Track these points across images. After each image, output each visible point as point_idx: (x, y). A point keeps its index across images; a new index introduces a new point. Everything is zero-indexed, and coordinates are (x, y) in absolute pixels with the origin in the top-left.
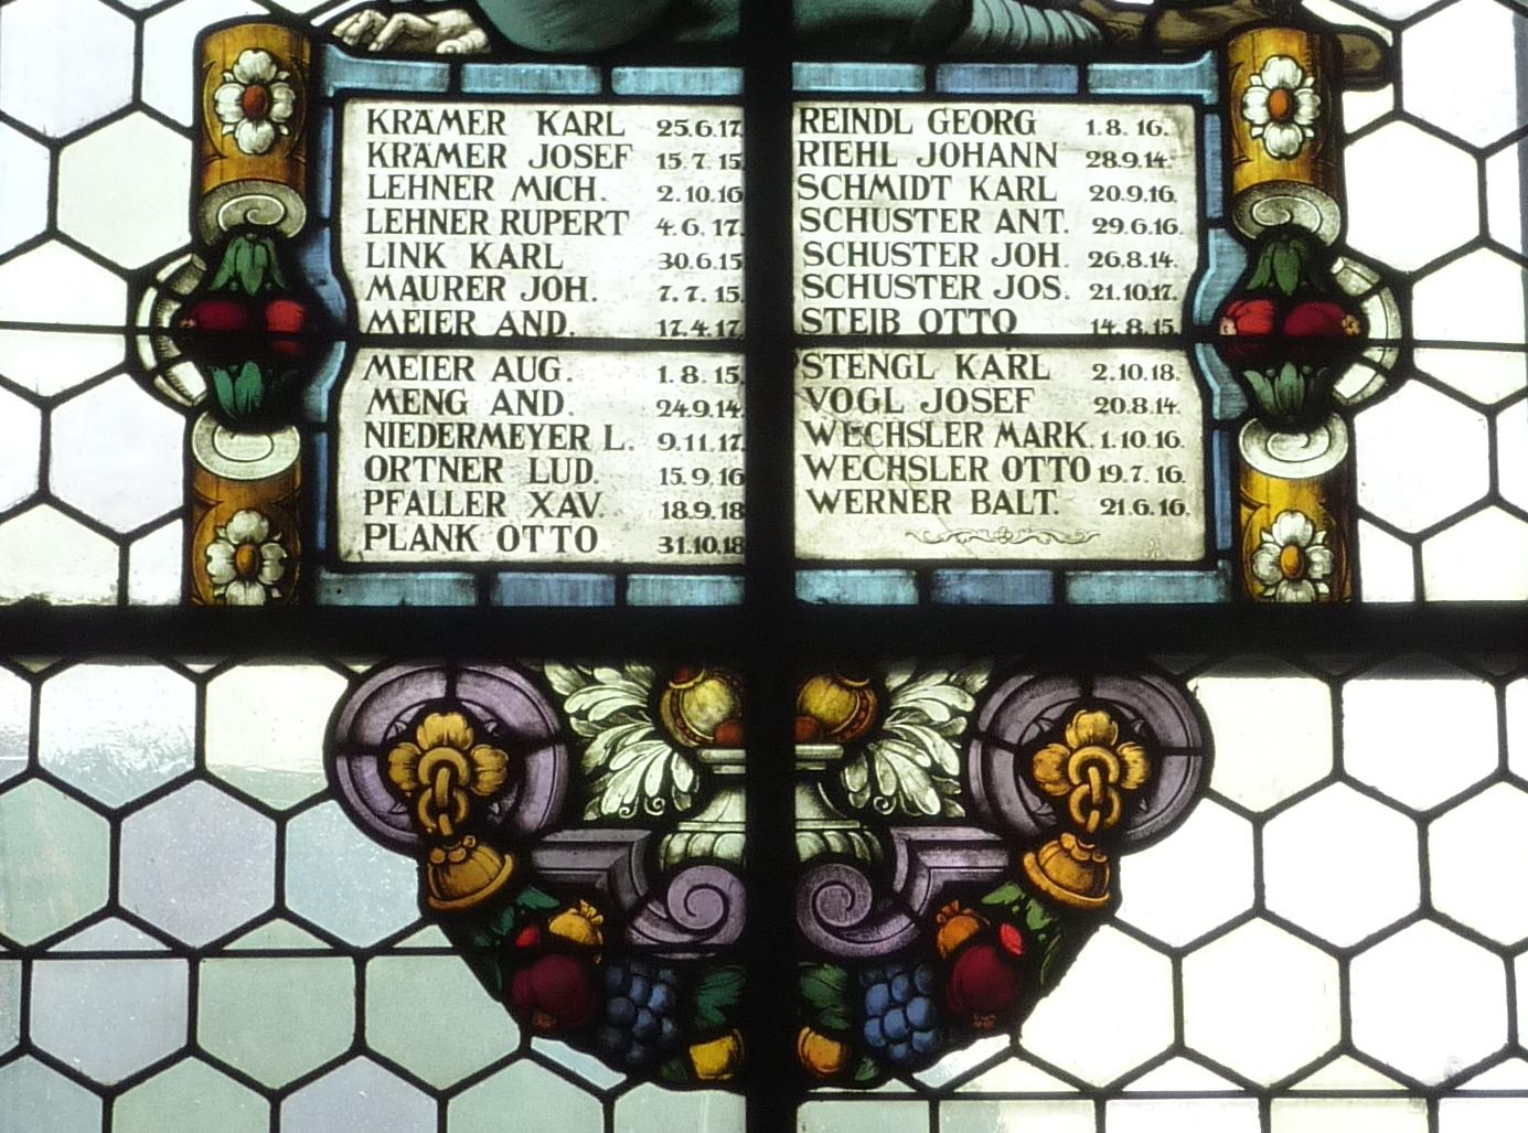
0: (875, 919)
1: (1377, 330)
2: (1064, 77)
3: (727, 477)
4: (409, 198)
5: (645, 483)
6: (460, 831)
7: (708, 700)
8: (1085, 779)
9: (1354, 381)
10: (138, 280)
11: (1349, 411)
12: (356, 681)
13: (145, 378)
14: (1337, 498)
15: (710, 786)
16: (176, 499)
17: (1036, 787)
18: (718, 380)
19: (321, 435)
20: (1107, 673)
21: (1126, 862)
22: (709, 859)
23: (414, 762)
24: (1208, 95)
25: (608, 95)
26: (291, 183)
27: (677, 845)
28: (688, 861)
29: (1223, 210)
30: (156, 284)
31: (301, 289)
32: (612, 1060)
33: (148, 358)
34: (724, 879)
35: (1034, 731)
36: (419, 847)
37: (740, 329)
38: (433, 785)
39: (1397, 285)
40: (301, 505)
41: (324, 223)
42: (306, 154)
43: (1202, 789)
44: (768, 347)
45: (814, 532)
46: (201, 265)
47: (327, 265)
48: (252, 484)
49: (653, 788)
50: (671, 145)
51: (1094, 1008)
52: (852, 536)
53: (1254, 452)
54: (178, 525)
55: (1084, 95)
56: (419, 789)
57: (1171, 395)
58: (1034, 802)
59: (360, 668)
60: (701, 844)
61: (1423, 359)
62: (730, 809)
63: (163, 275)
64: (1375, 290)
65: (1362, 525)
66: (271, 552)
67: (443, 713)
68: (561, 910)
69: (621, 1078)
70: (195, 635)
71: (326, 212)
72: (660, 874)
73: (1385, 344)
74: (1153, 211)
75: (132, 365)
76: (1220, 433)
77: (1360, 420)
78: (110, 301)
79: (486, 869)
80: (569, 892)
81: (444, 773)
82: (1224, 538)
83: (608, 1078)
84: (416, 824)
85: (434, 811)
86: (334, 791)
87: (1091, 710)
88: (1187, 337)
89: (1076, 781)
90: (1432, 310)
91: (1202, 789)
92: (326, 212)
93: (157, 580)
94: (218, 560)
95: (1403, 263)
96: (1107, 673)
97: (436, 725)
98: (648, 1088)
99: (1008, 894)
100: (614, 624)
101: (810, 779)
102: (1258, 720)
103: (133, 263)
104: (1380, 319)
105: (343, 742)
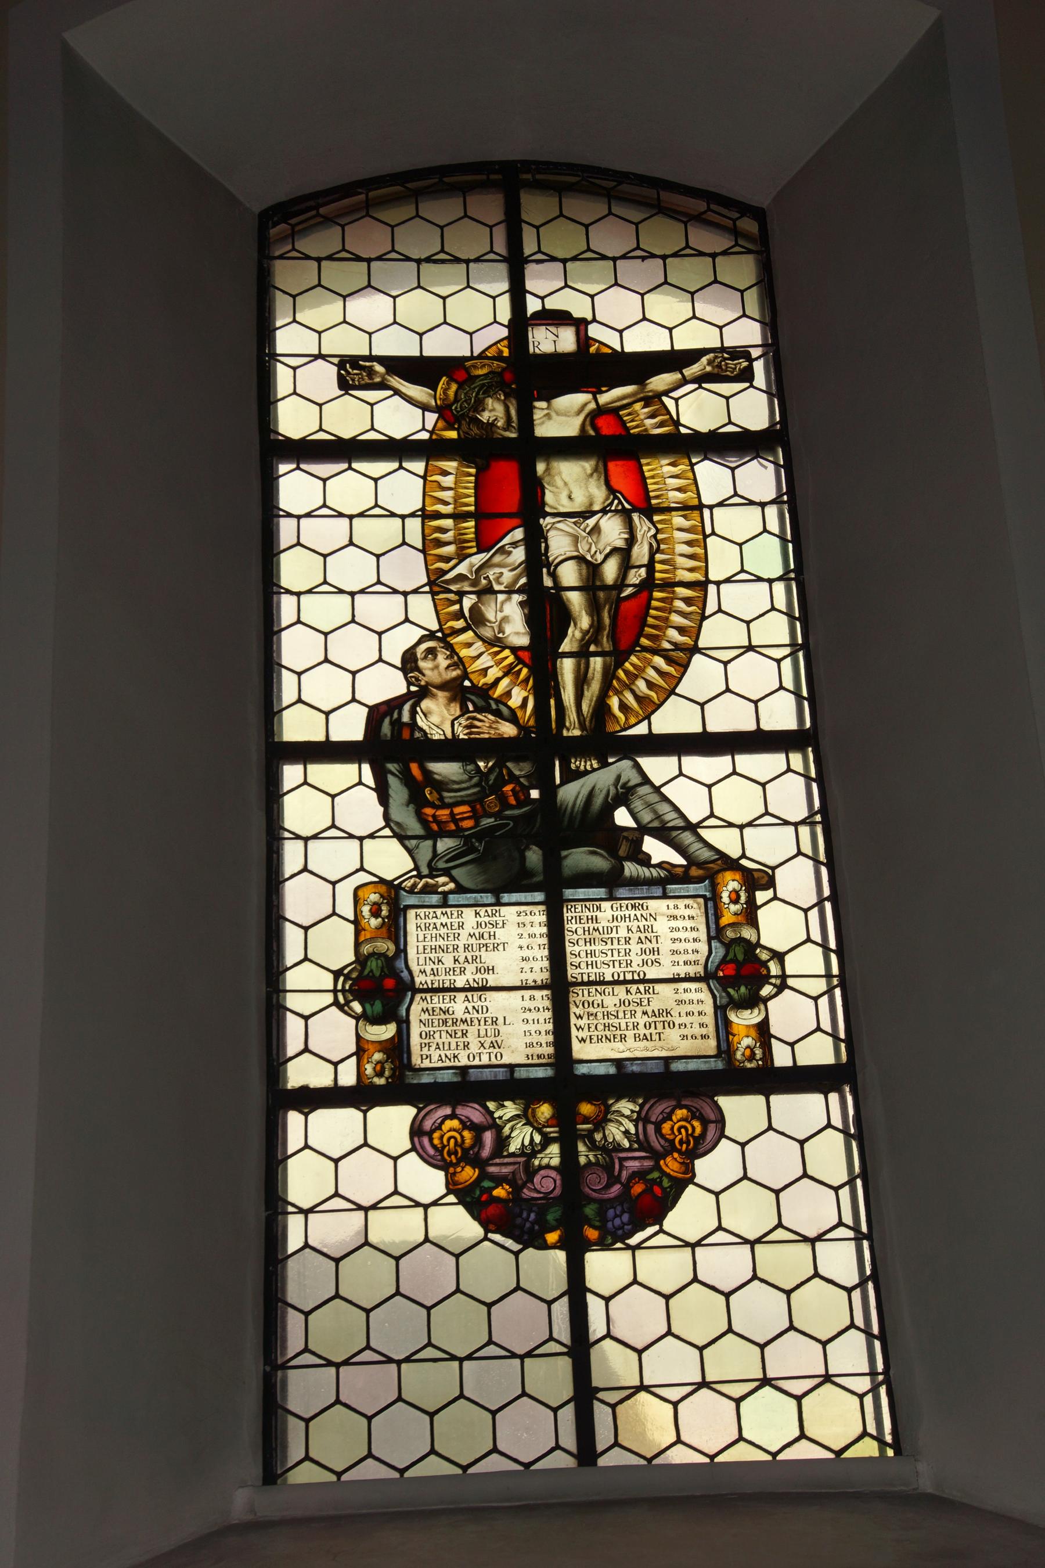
2: (658, 891)
5: (518, 1034)
6: (459, 1161)
7: (545, 1111)
8: (680, 1133)
9: (766, 990)
10: (337, 974)
11: (765, 1000)
12: (420, 1110)
13: (341, 1008)
17: (663, 1136)
18: (542, 999)
19: (404, 1026)
21: (699, 1163)
23: (442, 1137)
26: (390, 938)
27: (536, 1162)
28: (541, 1167)
31: (395, 974)
34: (553, 1174)
35: (661, 1117)
36: (442, 1166)
39: (780, 957)
40: (398, 1048)
41: (402, 951)
44: (559, 986)
45: (579, 1051)
46: (359, 967)
47: (403, 966)
48: (380, 1042)
49: (527, 1142)
50: (521, 919)
52: (591, 1050)
53: (732, 1016)
54: (354, 1059)
55: (665, 896)
56: (444, 1147)
58: (662, 1142)
60: (545, 1161)
61: (790, 982)
63: (346, 972)
65: (773, 1040)
69: (520, 1247)
70: (361, 1097)
72: (531, 1173)
73: (776, 977)
75: (336, 1003)
76: (720, 1011)
79: (468, 1174)
80: (499, 1181)
81: (452, 1141)
82: (724, 1046)
84: (443, 1159)
85: (449, 1154)
86: (413, 1149)
92: (402, 947)
93: (348, 1077)
94: (369, 1069)
95: (781, 948)
96: (686, 1096)
98: (530, 1251)
99: (655, 1175)
101: (582, 1138)
103: (335, 968)
104: (774, 969)
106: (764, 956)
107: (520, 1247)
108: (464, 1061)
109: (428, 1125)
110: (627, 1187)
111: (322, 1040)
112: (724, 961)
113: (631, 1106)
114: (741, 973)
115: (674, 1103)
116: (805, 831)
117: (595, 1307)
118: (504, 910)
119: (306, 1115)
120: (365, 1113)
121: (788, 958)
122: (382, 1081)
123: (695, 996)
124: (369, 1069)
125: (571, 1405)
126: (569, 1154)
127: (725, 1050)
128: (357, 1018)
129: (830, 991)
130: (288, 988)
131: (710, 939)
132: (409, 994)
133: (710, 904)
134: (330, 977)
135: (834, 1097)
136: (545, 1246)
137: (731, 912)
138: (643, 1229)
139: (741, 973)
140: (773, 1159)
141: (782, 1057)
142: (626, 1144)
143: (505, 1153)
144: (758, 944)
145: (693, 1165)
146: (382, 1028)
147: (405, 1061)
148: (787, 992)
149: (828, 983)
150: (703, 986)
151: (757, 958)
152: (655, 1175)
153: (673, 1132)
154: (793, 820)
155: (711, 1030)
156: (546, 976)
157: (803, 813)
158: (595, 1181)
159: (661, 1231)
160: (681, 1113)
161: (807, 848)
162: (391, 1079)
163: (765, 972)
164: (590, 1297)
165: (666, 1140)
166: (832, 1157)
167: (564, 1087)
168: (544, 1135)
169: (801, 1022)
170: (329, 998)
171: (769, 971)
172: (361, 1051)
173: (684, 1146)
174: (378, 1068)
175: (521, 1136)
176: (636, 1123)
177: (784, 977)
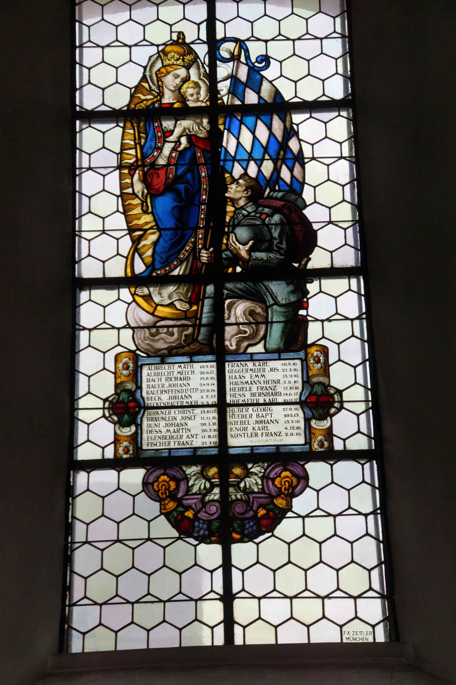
0: (246, 512)
1: (336, 400)
2: (276, 356)
3: (214, 424)
4: (156, 383)
5: (200, 432)
6: (167, 497)
7: (213, 471)
9: (333, 410)
11: (332, 416)
12: (148, 470)
13: (106, 418)
14: (329, 434)
15: (213, 486)
16: (112, 440)
17: (275, 486)
18: (213, 414)
19: (139, 426)
20: (288, 464)
22: (213, 500)
23: (158, 486)
24: (304, 358)
25: (192, 361)
27: (207, 498)
28: (210, 501)
29: (307, 381)
30: (109, 401)
31: (135, 400)
32: (196, 539)
33: (107, 414)
34: (217, 504)
36: (160, 500)
37: (216, 402)
38: (162, 489)
39: (340, 392)
40: (135, 439)
41: (140, 388)
42: (136, 376)
43: (307, 486)
44: (222, 406)
45: (232, 442)
48: (128, 436)
49: (202, 487)
51: (288, 528)
52: (238, 441)
53: (313, 423)
55: (280, 359)
56: (160, 490)
57: (298, 415)
59: (148, 468)
60: (211, 498)
61: (346, 405)
62: (217, 490)
63: (110, 399)
64: (335, 393)
65: (334, 438)
66: (131, 448)
67: (164, 476)
68: (186, 511)
69: (198, 542)
70: (117, 464)
71: (139, 385)
72: (204, 504)
73: (338, 402)
74: (293, 373)
76: (307, 421)
77: (334, 418)
78: (100, 404)
79: (171, 505)
80: (188, 508)
81: (164, 487)
83: (195, 543)
84: (159, 497)
85: (162, 494)
86: (143, 490)
87: (286, 471)
88: (301, 403)
89: (283, 484)
90: (346, 396)
91: (307, 486)
92: (139, 385)
93: (110, 453)
94: (121, 451)
95: (341, 388)
96: (288, 464)
97: (162, 478)
98: (202, 545)
100: (195, 457)
101: (233, 486)
102: (317, 471)
104: (336, 398)
105: (145, 484)
106: (332, 392)
107: (198, 542)
108: (172, 446)
109: (151, 480)
110: (256, 512)
111: (95, 434)
112: (310, 394)
113: (258, 469)
114: (320, 401)
115: (282, 468)
116: (357, 323)
117: (236, 575)
118: (195, 365)
119: (89, 473)
120: (119, 472)
121: (344, 393)
122: (128, 456)
123: (293, 412)
124: (121, 451)
125: (222, 625)
126: (224, 494)
127: (308, 442)
128: (115, 423)
129: (367, 411)
130: (80, 407)
131: (303, 382)
132: (142, 411)
133: (305, 362)
134: (102, 402)
135: (367, 466)
136: (211, 542)
137: (316, 368)
138: (263, 534)
139: (320, 401)
140: (333, 500)
141: (338, 445)
142: (256, 490)
143: (191, 493)
144: (329, 385)
145: (292, 502)
146: (128, 429)
147: (140, 445)
148: (343, 410)
149: (367, 405)
150: (298, 407)
151: (328, 392)
152: (271, 506)
153: (281, 484)
154: (351, 317)
155: (302, 431)
156: (215, 400)
157: (356, 314)
158: (239, 509)
159: (273, 535)
160: (284, 474)
161: (357, 333)
162: (132, 456)
163: (332, 400)
164: (233, 569)
165: (277, 488)
166: (365, 499)
167: (222, 459)
168: (211, 483)
169: (350, 426)
170: (100, 413)
171: (334, 399)
172: (117, 441)
173: (287, 492)
174: (126, 449)
175: (198, 485)
176: (262, 478)
177: (342, 402)
